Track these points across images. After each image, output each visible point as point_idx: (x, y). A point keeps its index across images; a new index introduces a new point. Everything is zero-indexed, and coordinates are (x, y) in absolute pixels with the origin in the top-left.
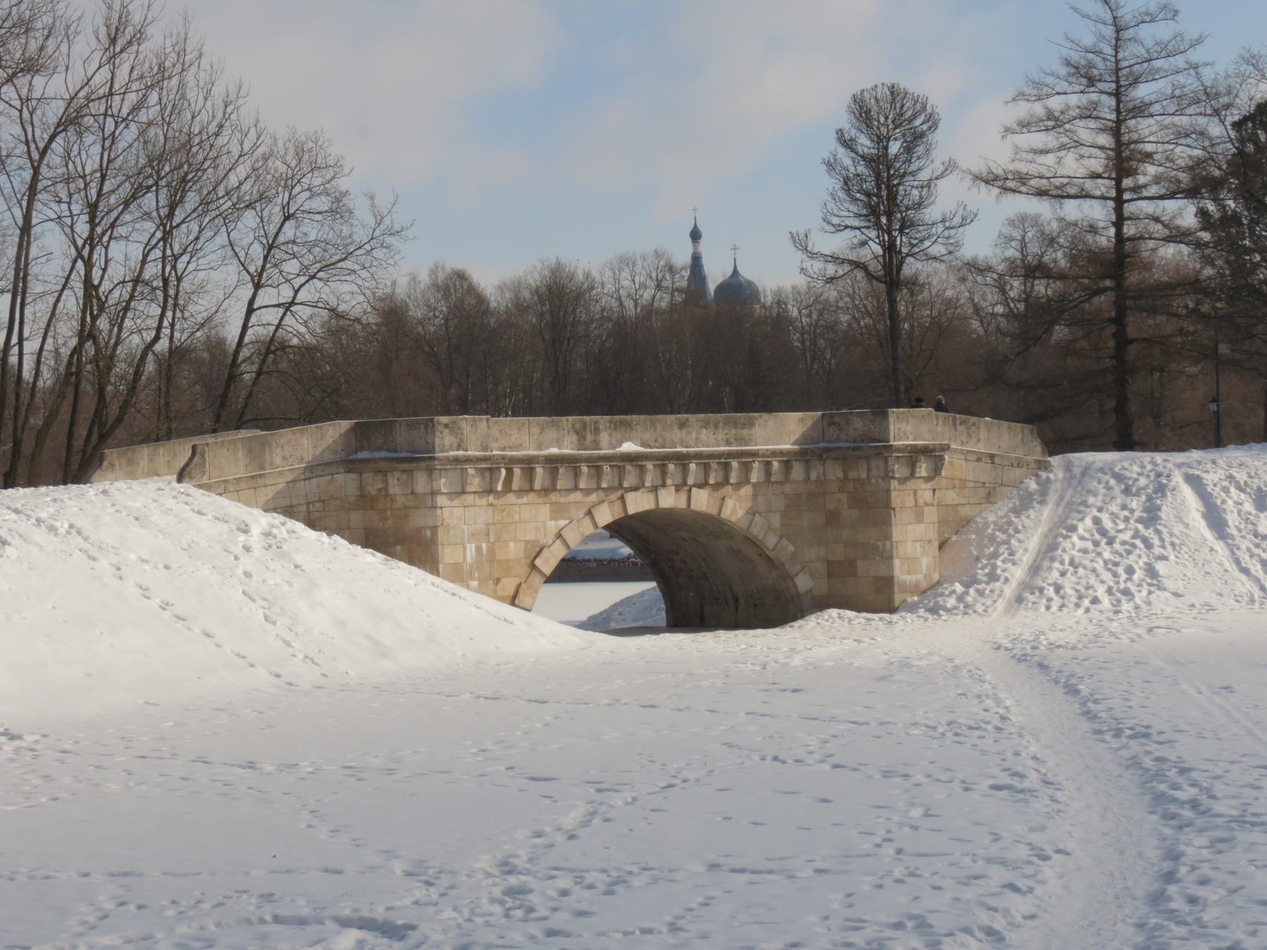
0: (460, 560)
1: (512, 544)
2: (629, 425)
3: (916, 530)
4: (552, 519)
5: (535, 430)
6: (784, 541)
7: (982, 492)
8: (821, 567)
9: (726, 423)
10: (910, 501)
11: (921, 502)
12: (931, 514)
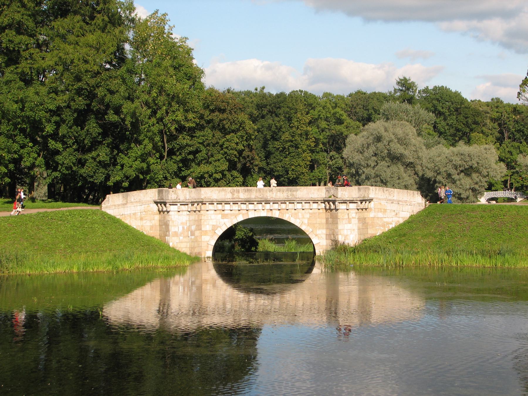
0: (177, 230)
1: (208, 226)
2: (251, 190)
3: (349, 226)
4: (222, 218)
5: (217, 192)
6: (309, 228)
7: (394, 214)
8: (324, 236)
9: (287, 190)
10: (346, 217)
11: (350, 217)
12: (355, 221)
